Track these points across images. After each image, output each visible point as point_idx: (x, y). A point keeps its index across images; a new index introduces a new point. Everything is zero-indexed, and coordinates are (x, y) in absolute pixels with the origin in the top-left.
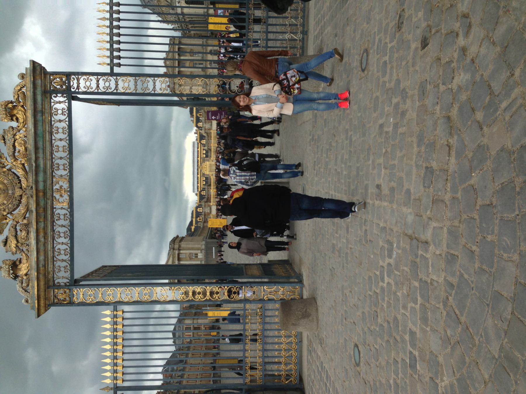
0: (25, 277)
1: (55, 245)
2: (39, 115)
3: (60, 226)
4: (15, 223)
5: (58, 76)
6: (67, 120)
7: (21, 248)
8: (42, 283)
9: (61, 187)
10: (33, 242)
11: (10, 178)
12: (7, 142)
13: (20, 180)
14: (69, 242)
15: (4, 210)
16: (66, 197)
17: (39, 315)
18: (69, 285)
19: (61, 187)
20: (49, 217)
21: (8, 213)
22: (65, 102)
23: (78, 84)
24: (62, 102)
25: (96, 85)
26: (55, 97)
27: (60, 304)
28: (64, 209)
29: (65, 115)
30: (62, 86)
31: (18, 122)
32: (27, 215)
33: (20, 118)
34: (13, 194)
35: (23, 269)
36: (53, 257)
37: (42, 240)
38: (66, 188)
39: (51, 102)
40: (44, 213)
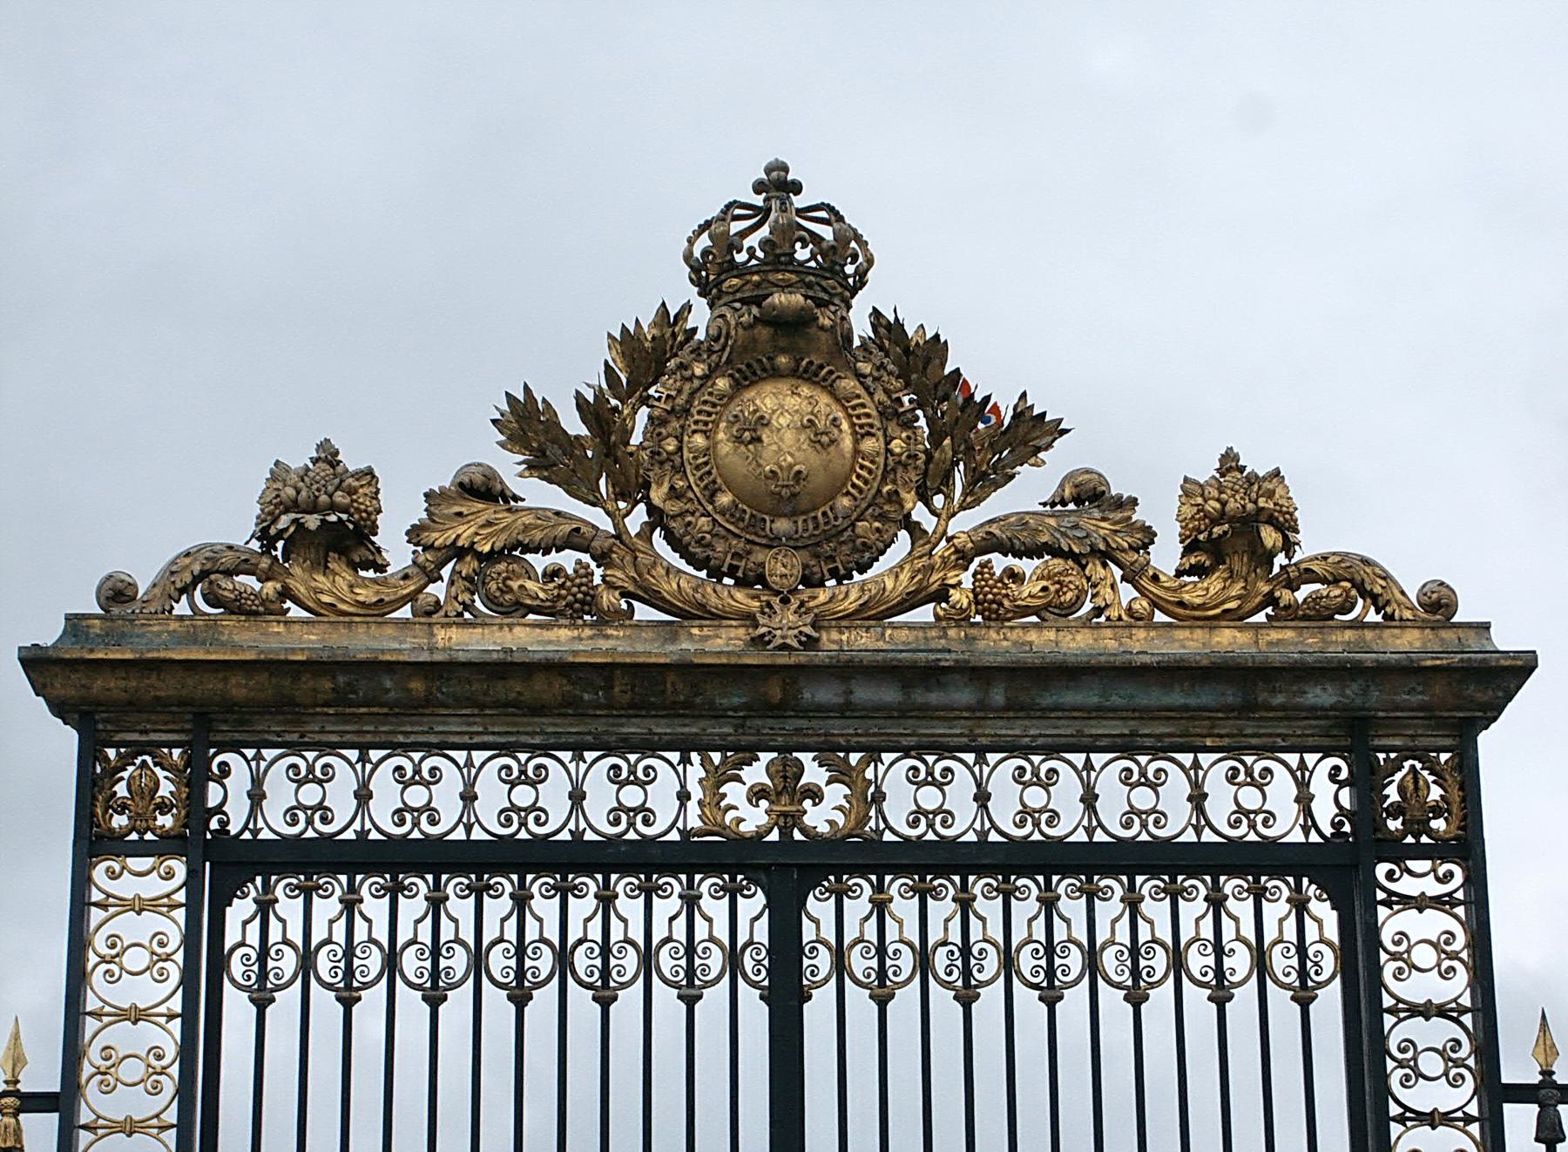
0: (271, 588)
1: (460, 756)
2: (1231, 697)
5: (1456, 795)
7: (446, 572)
8: (238, 688)
9: (815, 795)
15: (674, 493)
16: (753, 818)
17: (36, 663)
19: (815, 795)
20: (632, 728)
21: (652, 510)
23: (1421, 903)
24: (1308, 812)
28: (683, 805)
31: (1179, 574)
32: (643, 612)
34: (773, 542)
35: (322, 581)
39: (1302, 750)
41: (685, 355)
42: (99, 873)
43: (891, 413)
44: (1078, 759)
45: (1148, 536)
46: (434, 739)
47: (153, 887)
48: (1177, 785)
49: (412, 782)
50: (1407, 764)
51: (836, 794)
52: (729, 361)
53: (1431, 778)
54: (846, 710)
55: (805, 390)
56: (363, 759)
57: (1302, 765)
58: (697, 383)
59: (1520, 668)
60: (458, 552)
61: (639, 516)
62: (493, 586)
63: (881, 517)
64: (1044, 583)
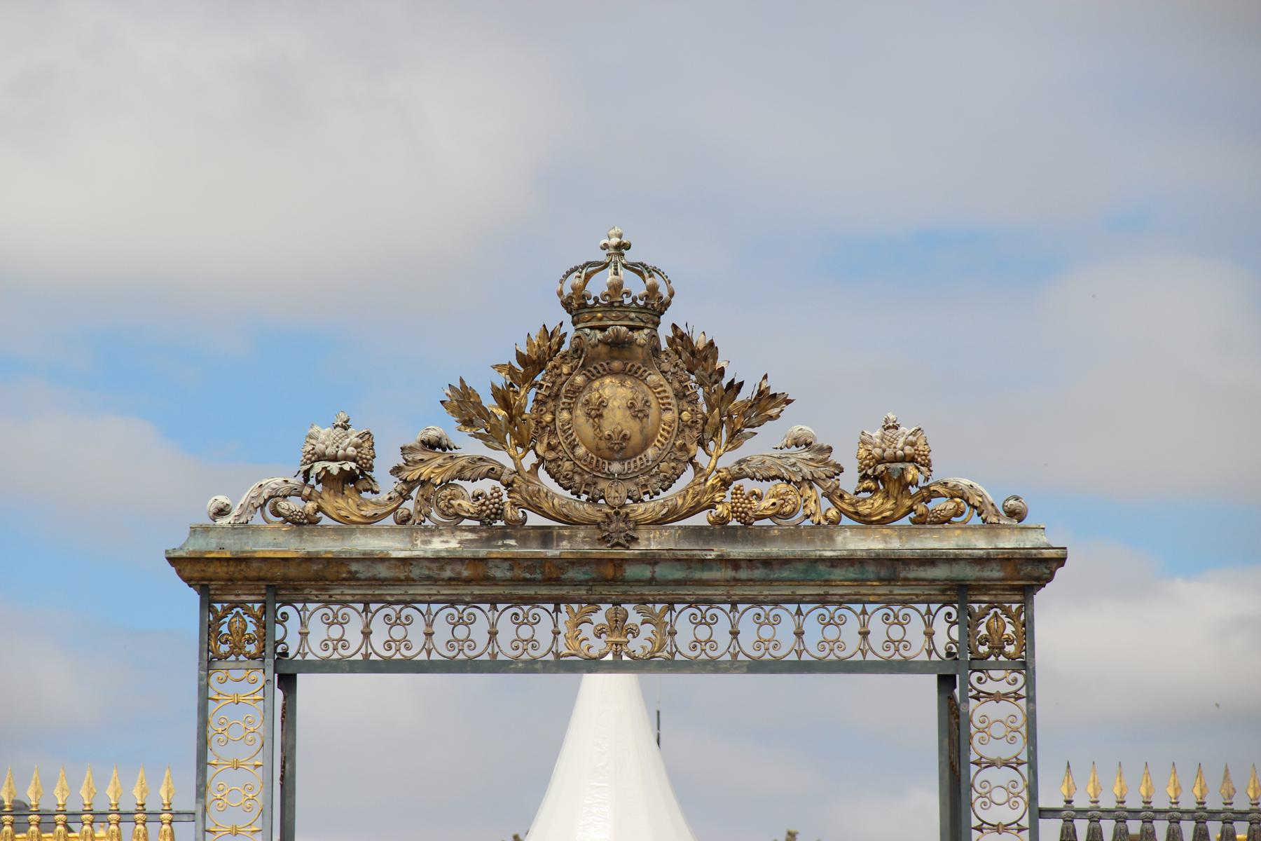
1: (423, 607)
3: (493, 625)
6: (870, 657)
7: (414, 494)
10: (441, 545)
15: (551, 448)
16: (598, 646)
19: (635, 632)
22: (929, 653)
25: (993, 757)
32: (534, 520)
34: (610, 476)
35: (341, 503)
37: (448, 573)
38: (631, 647)
39: (928, 602)
40: (539, 582)
41: (557, 360)
42: (213, 680)
43: (681, 395)
46: (408, 598)
48: (853, 625)
49: (395, 624)
50: (992, 612)
52: (583, 366)
53: (1007, 620)
54: (652, 582)
55: (629, 383)
56: (366, 610)
57: (929, 612)
58: (564, 378)
61: (530, 459)
62: (442, 504)
64: (773, 500)
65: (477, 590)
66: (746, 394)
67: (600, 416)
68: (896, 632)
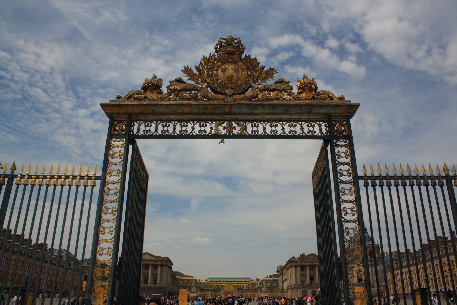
1: (173, 122)
4: (198, 89)
5: (347, 128)
9: (235, 128)
11: (243, 86)
12: (278, 85)
13: (241, 94)
14: (176, 134)
16: (224, 132)
18: (130, 134)
19: (235, 128)
22: (321, 134)
23: (341, 146)
26: (325, 125)
27: (112, 126)
28: (211, 130)
29: (309, 133)
30: (337, 131)
33: (301, 95)
34: (228, 88)
35: (152, 95)
36: (161, 121)
37: (180, 111)
38: (233, 132)
39: (320, 121)
44: (281, 123)
45: (292, 88)
46: (169, 119)
47: (121, 143)
51: (238, 128)
54: (240, 114)
59: (356, 106)
60: (175, 90)
62: (180, 95)
63: (246, 84)
65: (189, 117)
66: (266, 69)
67: (225, 71)
68: (311, 129)
